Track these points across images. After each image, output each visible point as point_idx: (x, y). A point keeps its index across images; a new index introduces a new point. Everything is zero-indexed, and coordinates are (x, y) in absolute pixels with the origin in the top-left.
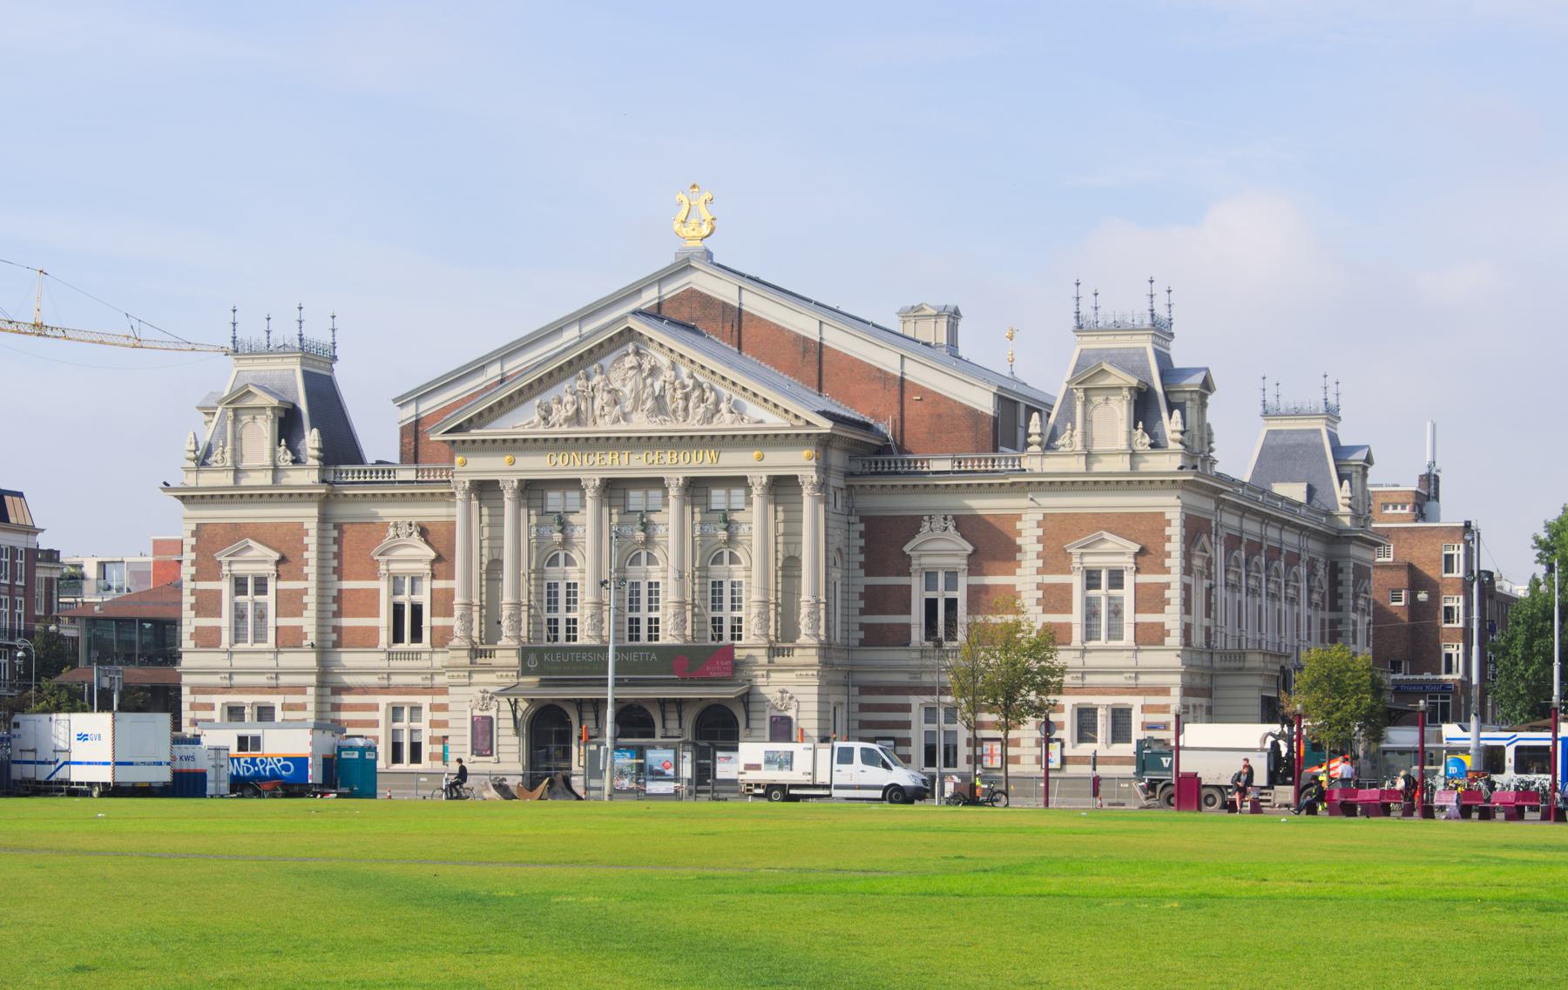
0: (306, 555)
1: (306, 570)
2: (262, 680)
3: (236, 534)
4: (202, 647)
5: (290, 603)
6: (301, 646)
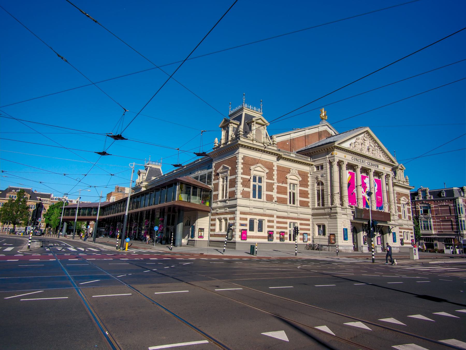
0: (274, 173)
1: (274, 177)
2: (261, 211)
3: (256, 162)
4: (244, 198)
5: (270, 187)
6: (272, 202)
